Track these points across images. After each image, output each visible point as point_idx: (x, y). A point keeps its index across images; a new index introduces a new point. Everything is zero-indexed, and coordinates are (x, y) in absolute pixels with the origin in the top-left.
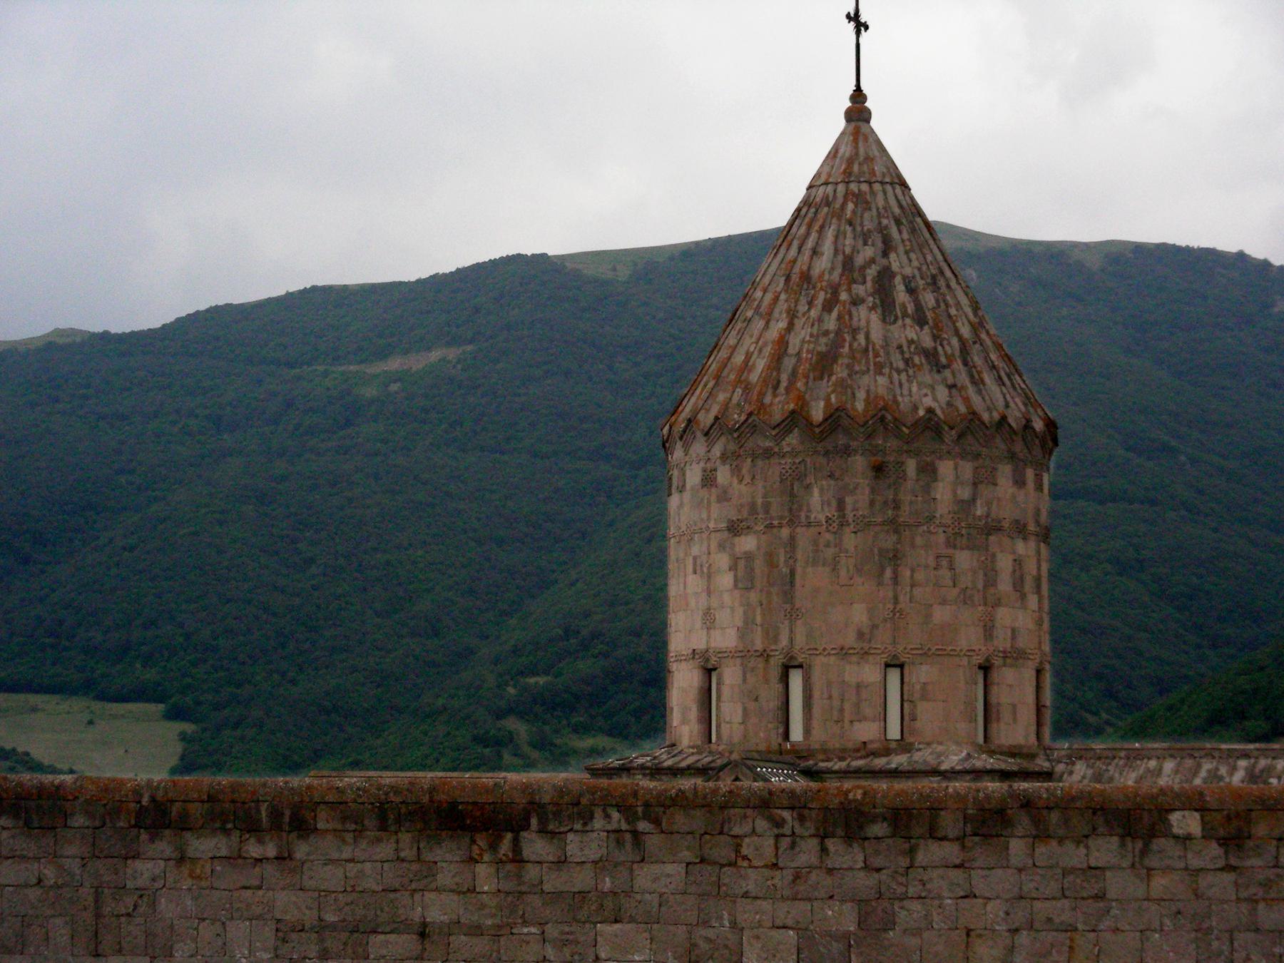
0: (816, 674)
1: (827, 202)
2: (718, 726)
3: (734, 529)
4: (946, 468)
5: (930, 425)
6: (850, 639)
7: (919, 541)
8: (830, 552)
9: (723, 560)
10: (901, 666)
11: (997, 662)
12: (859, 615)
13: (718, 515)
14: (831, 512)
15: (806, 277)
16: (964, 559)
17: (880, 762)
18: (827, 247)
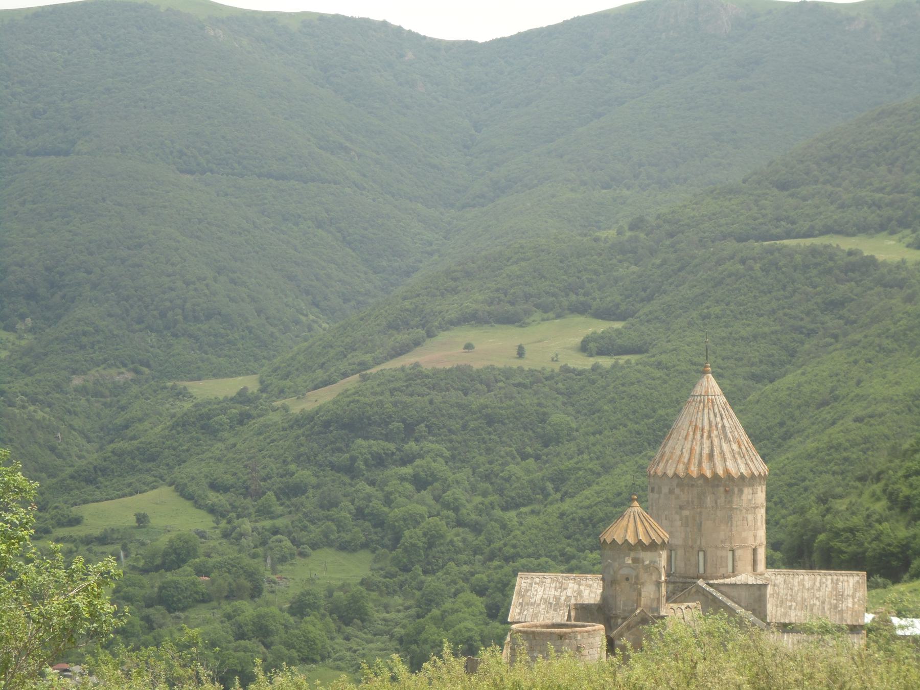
3: (681, 508)
9: (677, 517)
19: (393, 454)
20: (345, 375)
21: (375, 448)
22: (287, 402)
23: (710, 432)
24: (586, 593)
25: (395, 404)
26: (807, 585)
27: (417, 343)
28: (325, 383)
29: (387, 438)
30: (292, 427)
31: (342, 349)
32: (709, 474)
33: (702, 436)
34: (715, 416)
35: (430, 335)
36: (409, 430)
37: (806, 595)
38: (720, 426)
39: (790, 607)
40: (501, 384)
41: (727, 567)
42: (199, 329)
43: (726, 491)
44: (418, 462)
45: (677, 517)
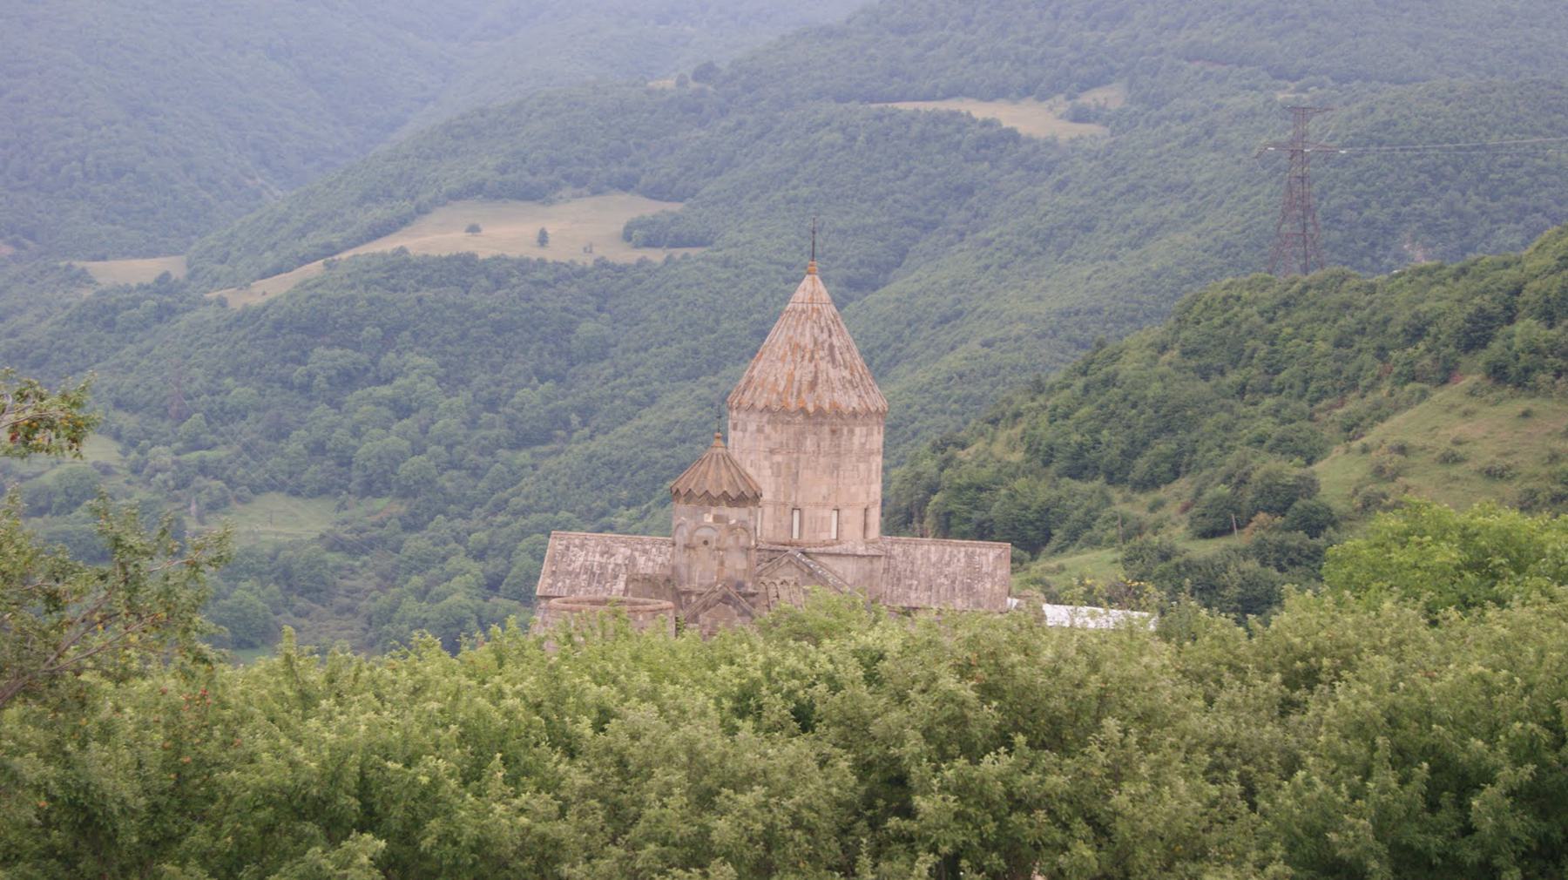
1: (803, 311)
3: (772, 452)
4: (857, 430)
5: (855, 414)
6: (820, 499)
9: (767, 464)
12: (824, 490)
13: (763, 445)
15: (798, 345)
16: (862, 466)
17: (830, 549)
18: (808, 334)
19: (367, 370)
20: (304, 260)
21: (341, 361)
22: (225, 293)
23: (812, 352)
24: (641, 560)
25: (371, 302)
26: (934, 559)
27: (402, 222)
28: (278, 271)
29: (357, 347)
30: (229, 327)
31: (300, 225)
32: (811, 408)
35: (421, 211)
36: (389, 337)
37: (932, 571)
39: (910, 587)
40: (514, 281)
42: (104, 191)
43: (833, 432)
44: (399, 381)
45: (767, 464)
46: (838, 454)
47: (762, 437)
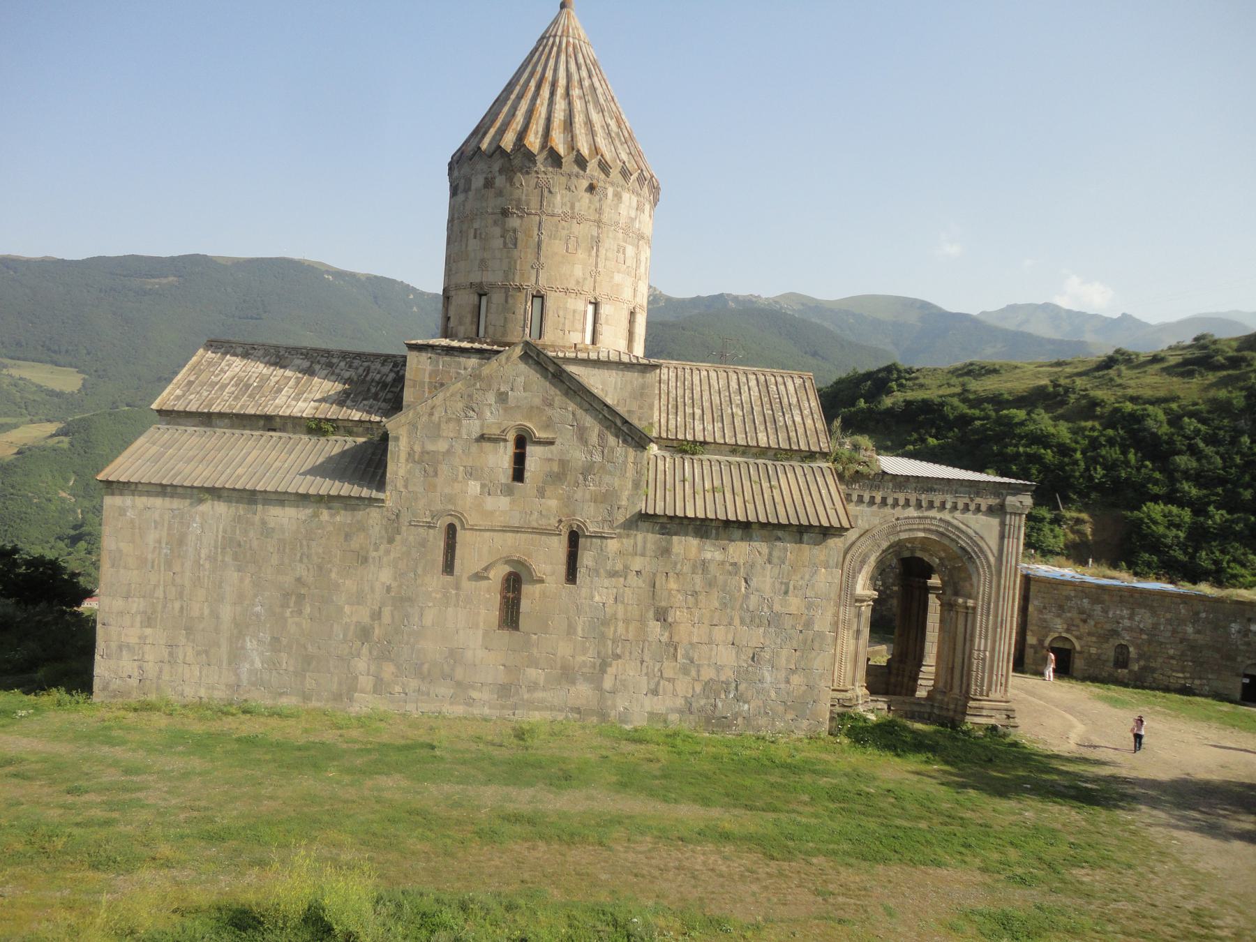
0: (549, 303)
2: (486, 328)
4: (626, 196)
6: (572, 285)
7: (611, 235)
8: (565, 232)
9: (497, 231)
10: (596, 305)
11: (637, 310)
14: (567, 209)
17: (581, 355)
33: (552, 93)
34: (579, 68)
38: (586, 83)
41: (584, 331)
45: (497, 231)
46: (599, 223)
47: (491, 193)
